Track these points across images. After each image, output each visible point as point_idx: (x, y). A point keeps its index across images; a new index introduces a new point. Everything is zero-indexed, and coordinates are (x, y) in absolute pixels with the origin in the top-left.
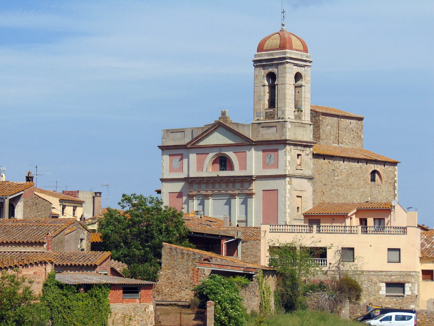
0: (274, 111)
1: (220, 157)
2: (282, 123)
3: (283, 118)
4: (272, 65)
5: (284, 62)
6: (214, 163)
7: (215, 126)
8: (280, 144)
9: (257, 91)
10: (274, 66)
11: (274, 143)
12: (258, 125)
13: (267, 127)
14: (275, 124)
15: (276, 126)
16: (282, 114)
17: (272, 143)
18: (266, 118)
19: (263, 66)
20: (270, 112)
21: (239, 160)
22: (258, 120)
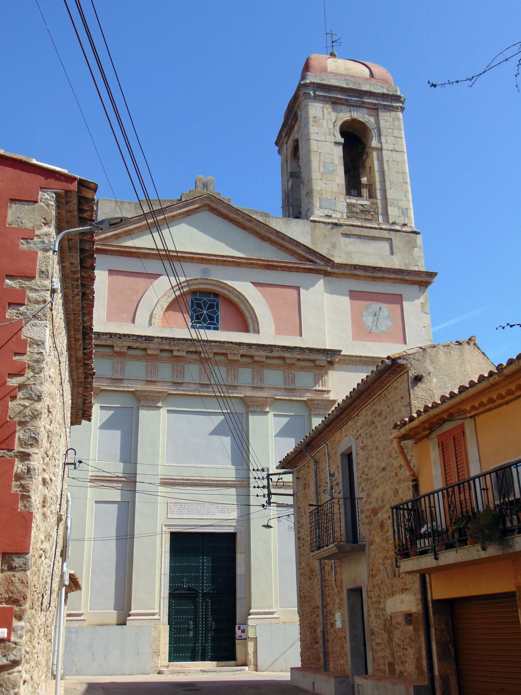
0: (374, 207)
1: (194, 293)
2: (408, 236)
3: (405, 225)
4: (361, 106)
5: (397, 108)
6: (174, 306)
7: (193, 203)
8: (407, 282)
9: (319, 151)
10: (365, 110)
11: (392, 276)
12: (332, 229)
13: (360, 237)
14: (385, 234)
15: (390, 240)
16: (401, 215)
17: (386, 275)
18: (348, 217)
19: (335, 102)
20: (362, 205)
21: (273, 308)
22: (329, 217)
